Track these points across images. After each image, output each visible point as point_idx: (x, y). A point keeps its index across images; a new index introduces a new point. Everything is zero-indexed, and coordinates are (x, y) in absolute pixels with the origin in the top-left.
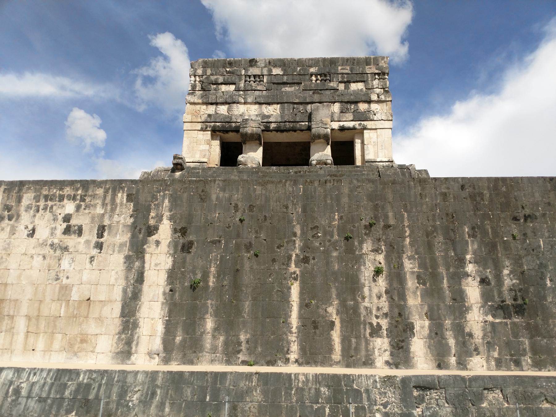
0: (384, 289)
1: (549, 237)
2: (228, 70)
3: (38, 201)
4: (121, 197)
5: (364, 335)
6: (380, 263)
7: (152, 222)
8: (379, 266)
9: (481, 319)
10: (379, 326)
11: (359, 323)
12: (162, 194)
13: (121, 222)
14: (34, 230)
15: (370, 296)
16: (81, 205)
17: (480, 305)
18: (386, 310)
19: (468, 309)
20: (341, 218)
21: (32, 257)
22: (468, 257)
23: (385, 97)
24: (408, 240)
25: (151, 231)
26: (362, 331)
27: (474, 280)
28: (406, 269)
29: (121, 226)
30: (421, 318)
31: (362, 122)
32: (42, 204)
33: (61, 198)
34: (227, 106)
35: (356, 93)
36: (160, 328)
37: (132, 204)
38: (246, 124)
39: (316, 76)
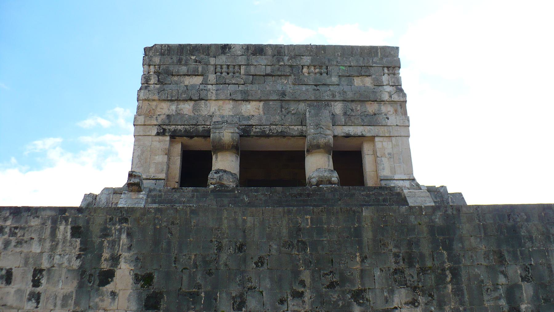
7: (105, 266)
13: (64, 266)
16: (11, 240)
23: (399, 96)
24: (450, 287)
25: (107, 277)
29: (64, 271)
34: (192, 103)
37: (79, 240)
39: (308, 67)
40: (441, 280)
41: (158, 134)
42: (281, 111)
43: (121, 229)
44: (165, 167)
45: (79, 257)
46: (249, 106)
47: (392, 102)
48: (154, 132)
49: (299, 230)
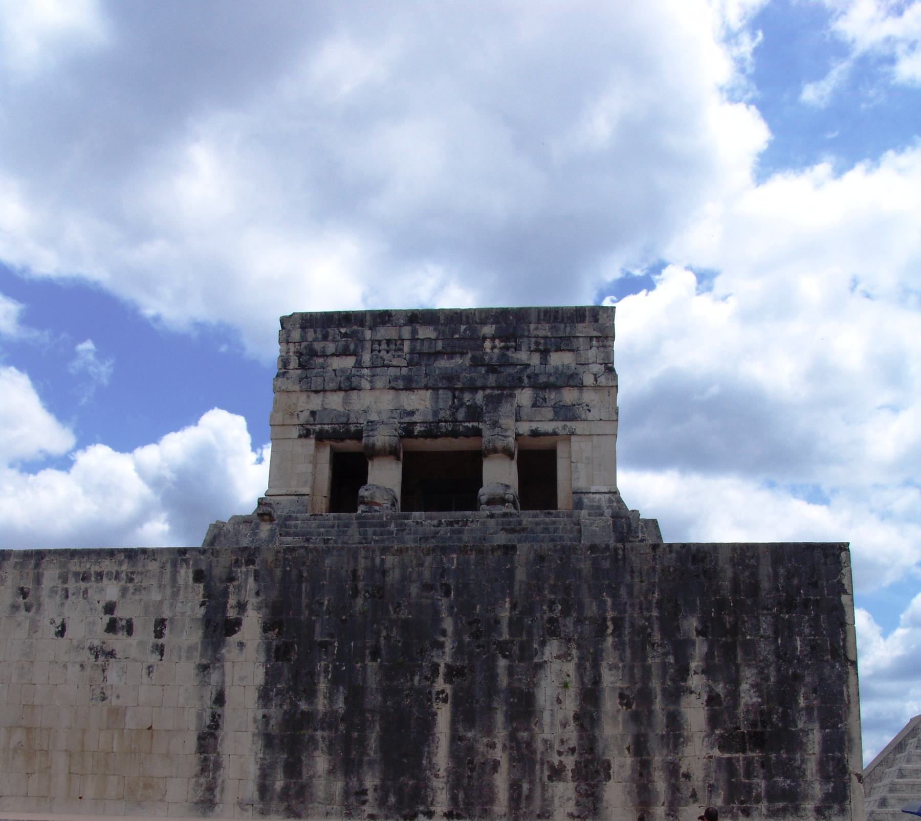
0: (572, 714)
2: (343, 330)
4: (186, 574)
5: (541, 779)
6: (568, 676)
7: (232, 614)
8: (568, 679)
11: (532, 762)
12: (244, 569)
13: (187, 614)
17: (704, 734)
18: (573, 743)
19: (687, 740)
20: (514, 606)
21: (65, 666)
22: (693, 665)
23: (607, 379)
24: (610, 640)
25: (232, 626)
26: (538, 772)
31: (568, 424)
32: (72, 585)
33: (100, 576)
34: (341, 394)
35: (557, 373)
36: (253, 770)
37: (202, 585)
38: (372, 430)
40: (601, 631)
41: (300, 436)
42: (454, 402)
43: (247, 571)
44: (310, 479)
46: (413, 397)
47: (597, 387)
48: (296, 435)
49: (444, 570)
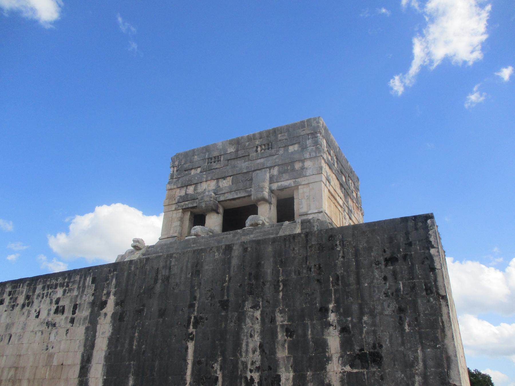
1: (410, 279)
3: (44, 290)
6: (258, 319)
7: (104, 298)
9: (340, 370)
10: (252, 379)
12: (112, 274)
14: (39, 312)
15: (247, 351)
17: (339, 355)
18: (258, 364)
24: (281, 294)
27: (335, 329)
28: (278, 323)
29: (86, 303)
30: (287, 370)
31: (297, 180)
41: (176, 209)
45: (93, 295)
